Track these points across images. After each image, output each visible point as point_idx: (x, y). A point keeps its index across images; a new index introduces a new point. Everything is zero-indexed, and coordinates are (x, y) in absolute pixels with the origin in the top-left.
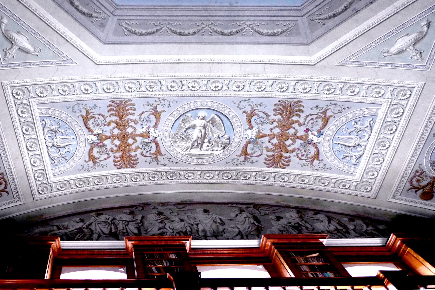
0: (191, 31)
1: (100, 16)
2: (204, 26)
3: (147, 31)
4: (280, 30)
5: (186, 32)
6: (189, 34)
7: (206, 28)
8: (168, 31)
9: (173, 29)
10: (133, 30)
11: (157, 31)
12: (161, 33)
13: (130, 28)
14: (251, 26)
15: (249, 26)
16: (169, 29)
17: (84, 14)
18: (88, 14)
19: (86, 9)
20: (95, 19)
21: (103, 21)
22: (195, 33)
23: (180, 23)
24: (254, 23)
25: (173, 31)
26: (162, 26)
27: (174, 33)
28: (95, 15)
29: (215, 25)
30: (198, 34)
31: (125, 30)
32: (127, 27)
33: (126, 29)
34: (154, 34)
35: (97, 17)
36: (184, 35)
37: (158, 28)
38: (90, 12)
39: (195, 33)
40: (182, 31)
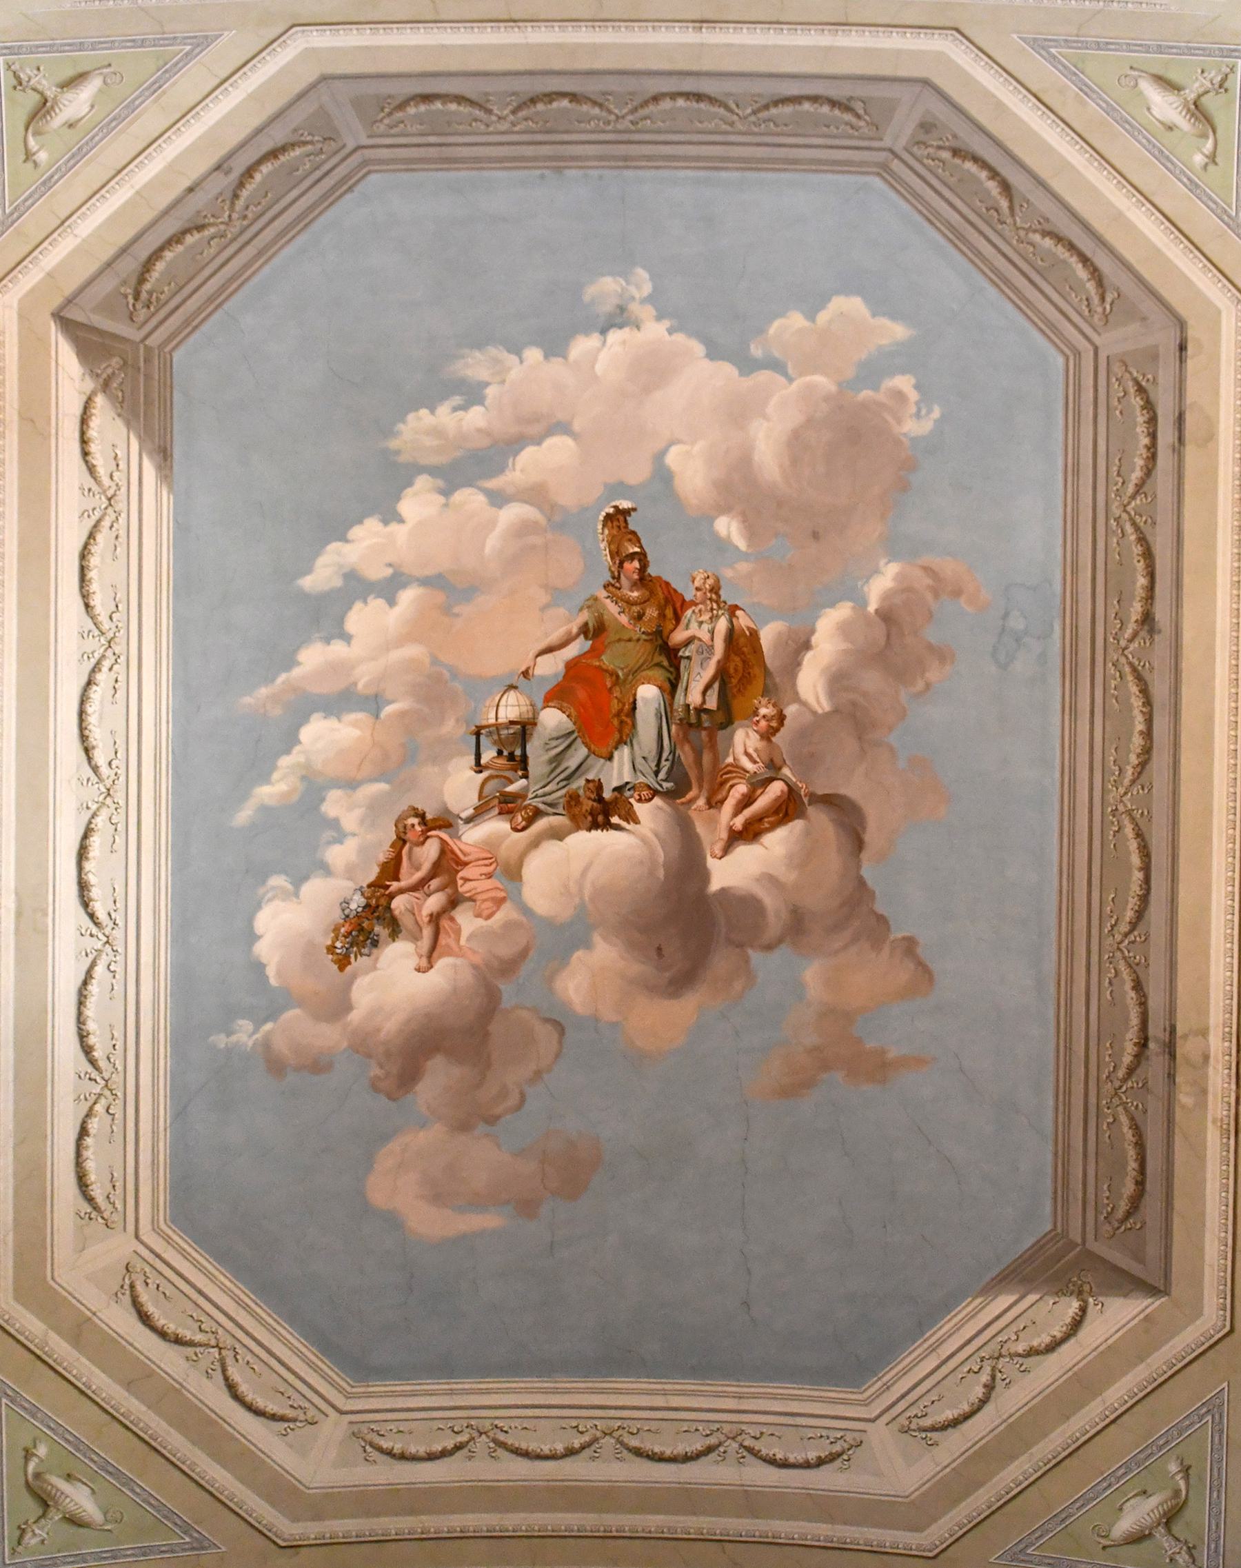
0: (666, 104)
1: (930, 150)
2: (630, 117)
3: (798, 107)
4: (411, 110)
5: (681, 102)
6: (674, 96)
7: (625, 111)
8: (733, 106)
9: (722, 111)
10: (837, 112)
11: (766, 107)
12: (756, 102)
13: (847, 117)
14: (494, 118)
15: (500, 118)
16: (731, 111)
17: (976, 159)
18: (964, 158)
19: (968, 171)
20: (947, 144)
21: (922, 137)
22: (656, 99)
23: (699, 125)
24: (488, 126)
25: (719, 106)
26: (753, 118)
27: (716, 101)
28: (946, 155)
29: (599, 120)
30: (648, 96)
31: (861, 112)
32: (854, 120)
33: (858, 116)
34: (775, 98)
35: (940, 148)
36: (687, 95)
37: (764, 115)
38: (957, 161)
39: (656, 99)
40: (695, 105)
